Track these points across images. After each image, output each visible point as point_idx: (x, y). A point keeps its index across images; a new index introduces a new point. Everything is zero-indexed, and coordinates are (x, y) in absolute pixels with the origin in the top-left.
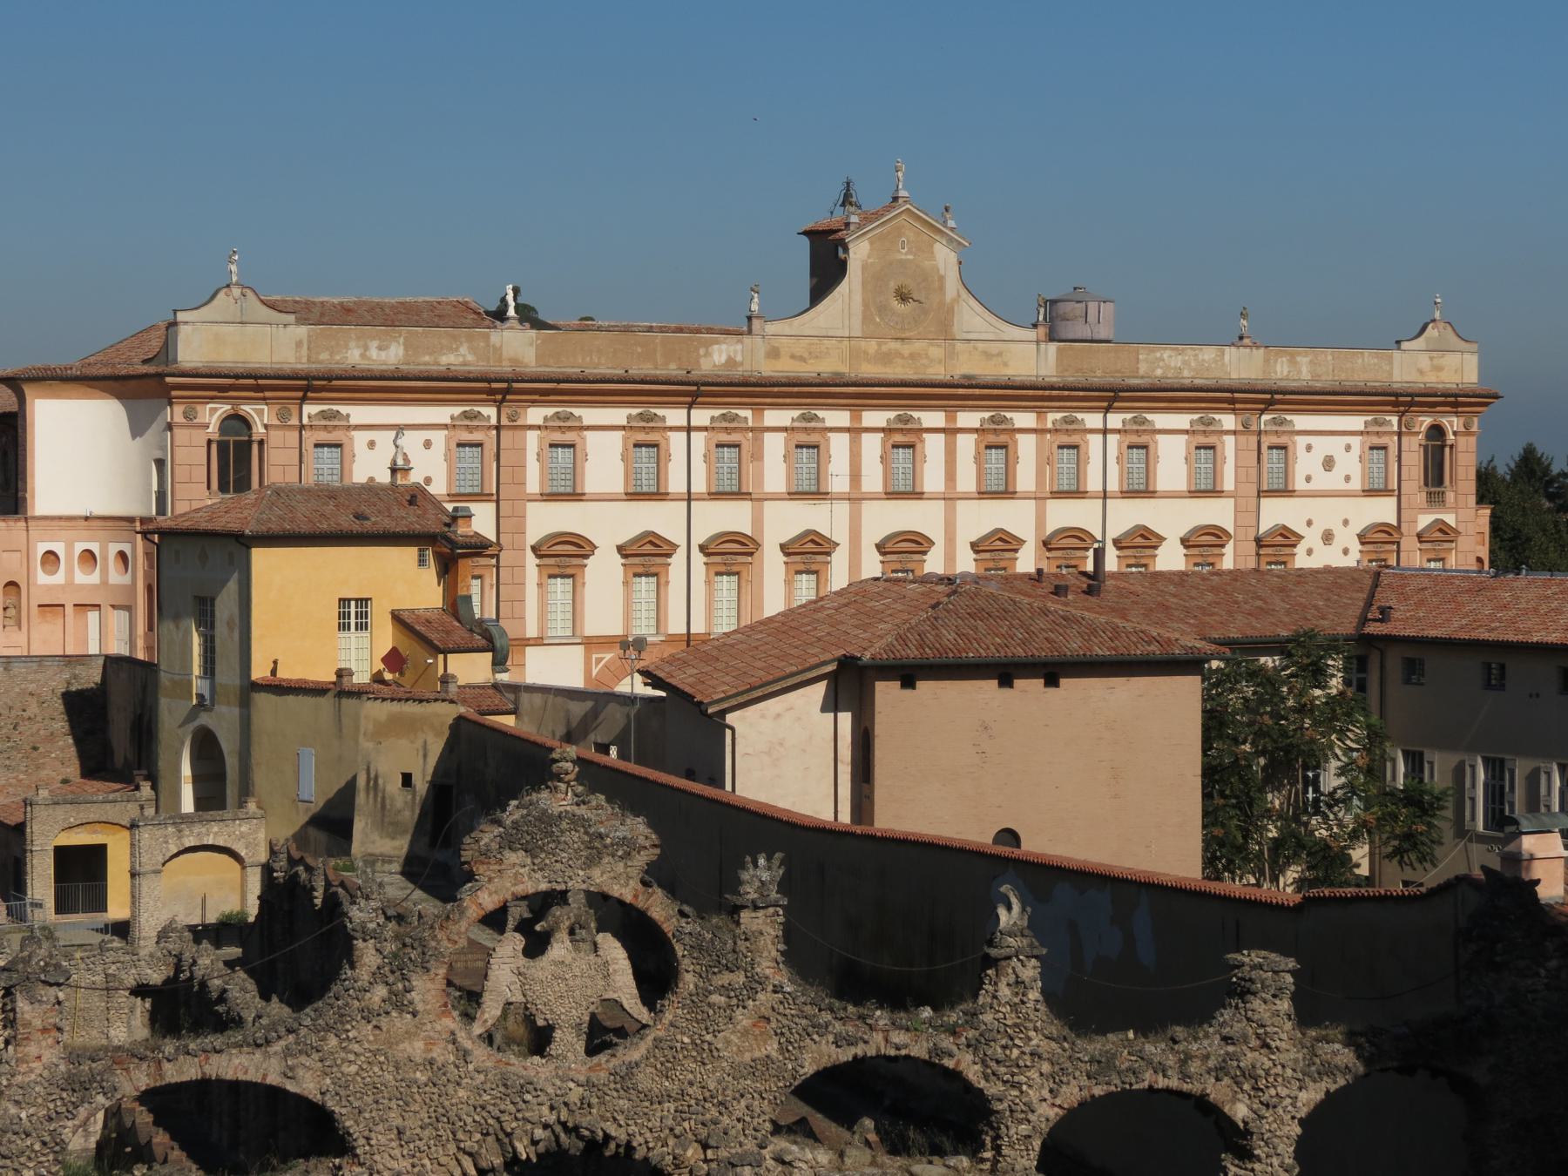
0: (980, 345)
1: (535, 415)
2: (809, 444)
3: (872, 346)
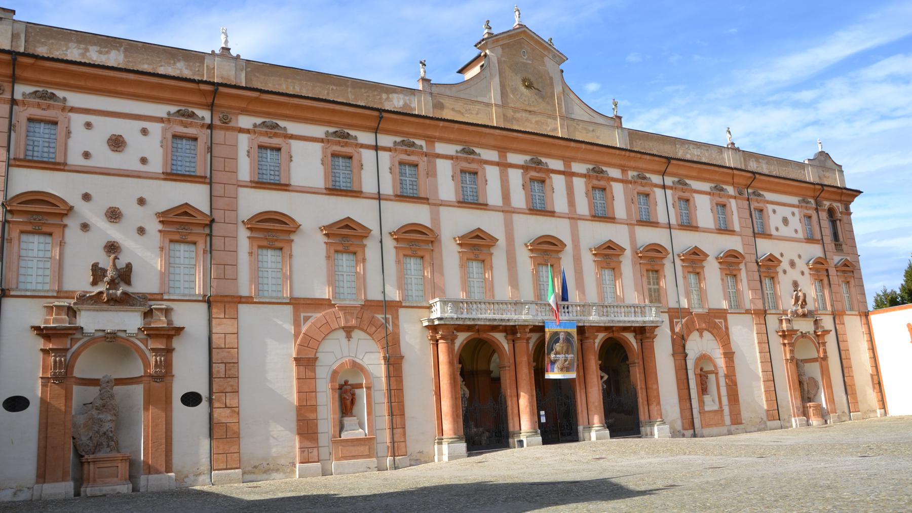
1: (245, 121)
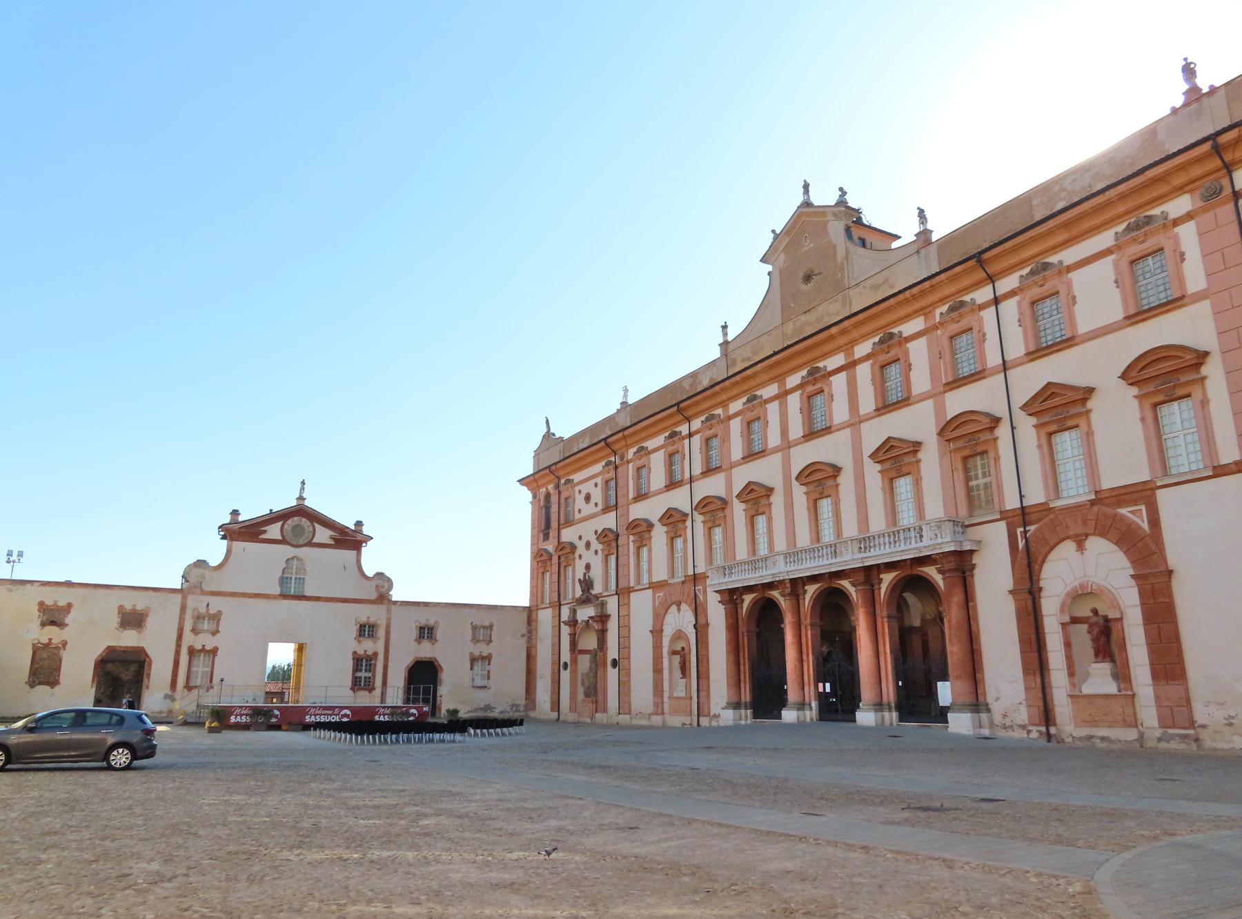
0: (869, 283)
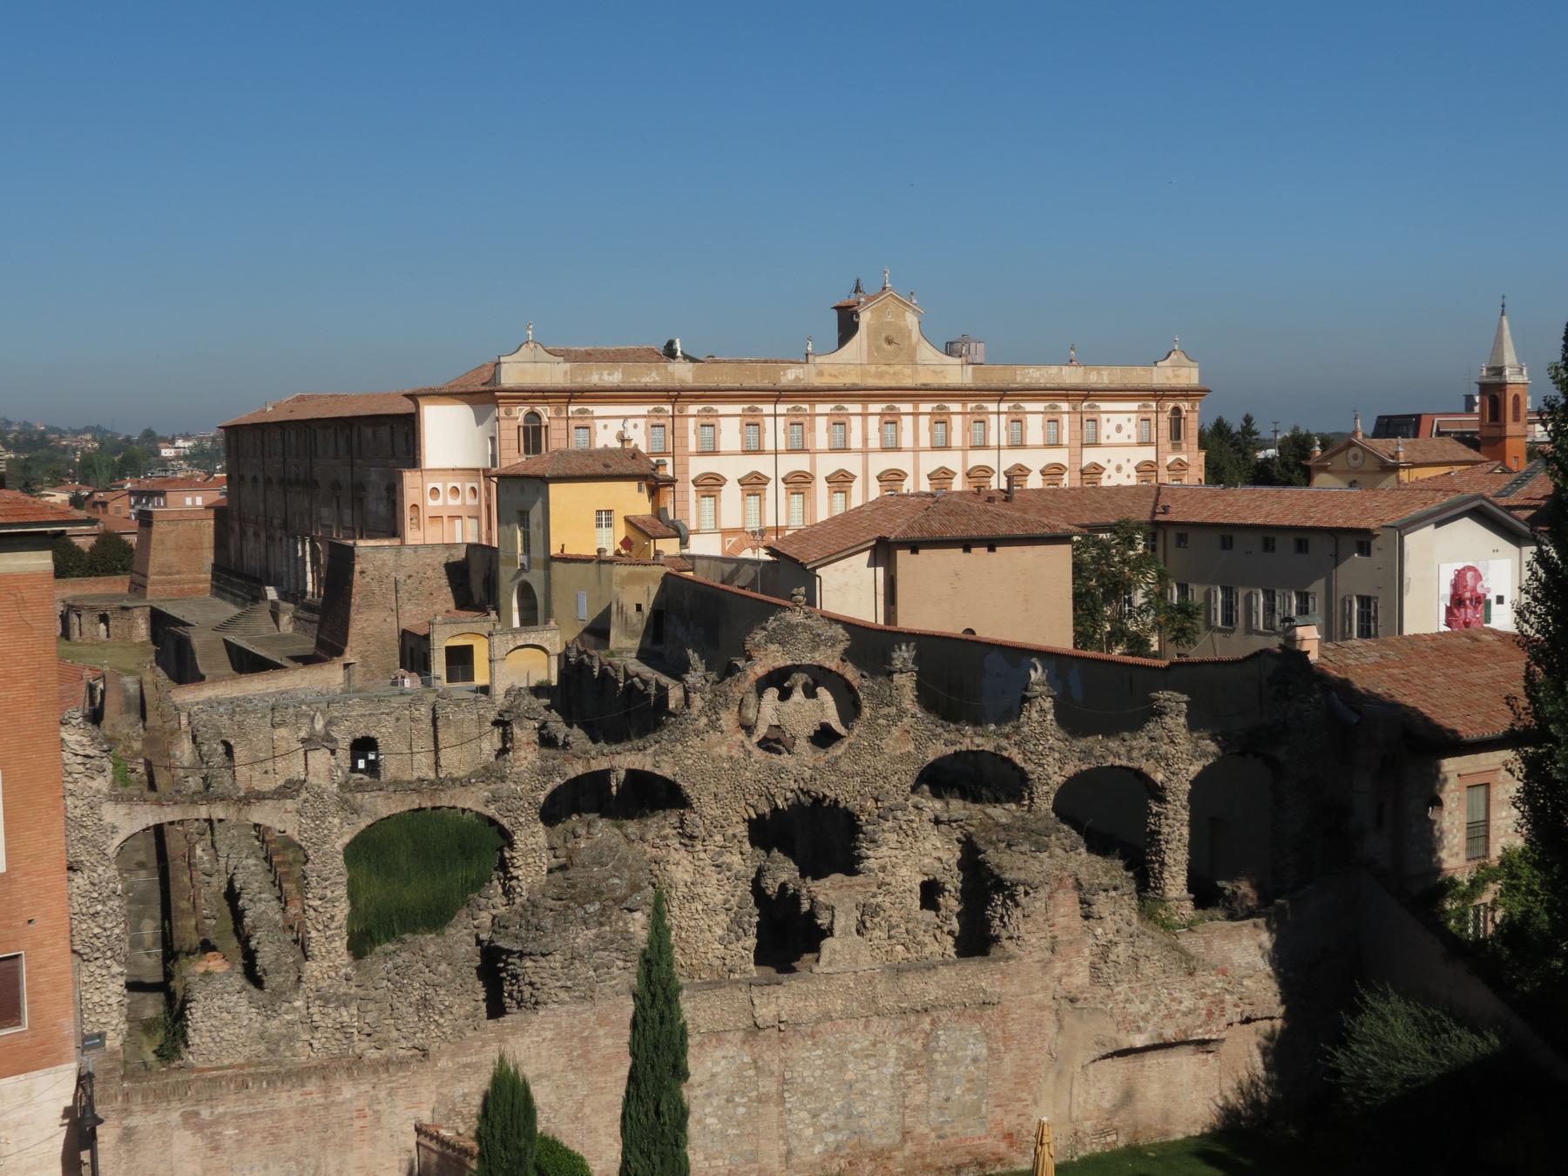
1: (693, 409)
2: (840, 422)
3: (873, 368)
